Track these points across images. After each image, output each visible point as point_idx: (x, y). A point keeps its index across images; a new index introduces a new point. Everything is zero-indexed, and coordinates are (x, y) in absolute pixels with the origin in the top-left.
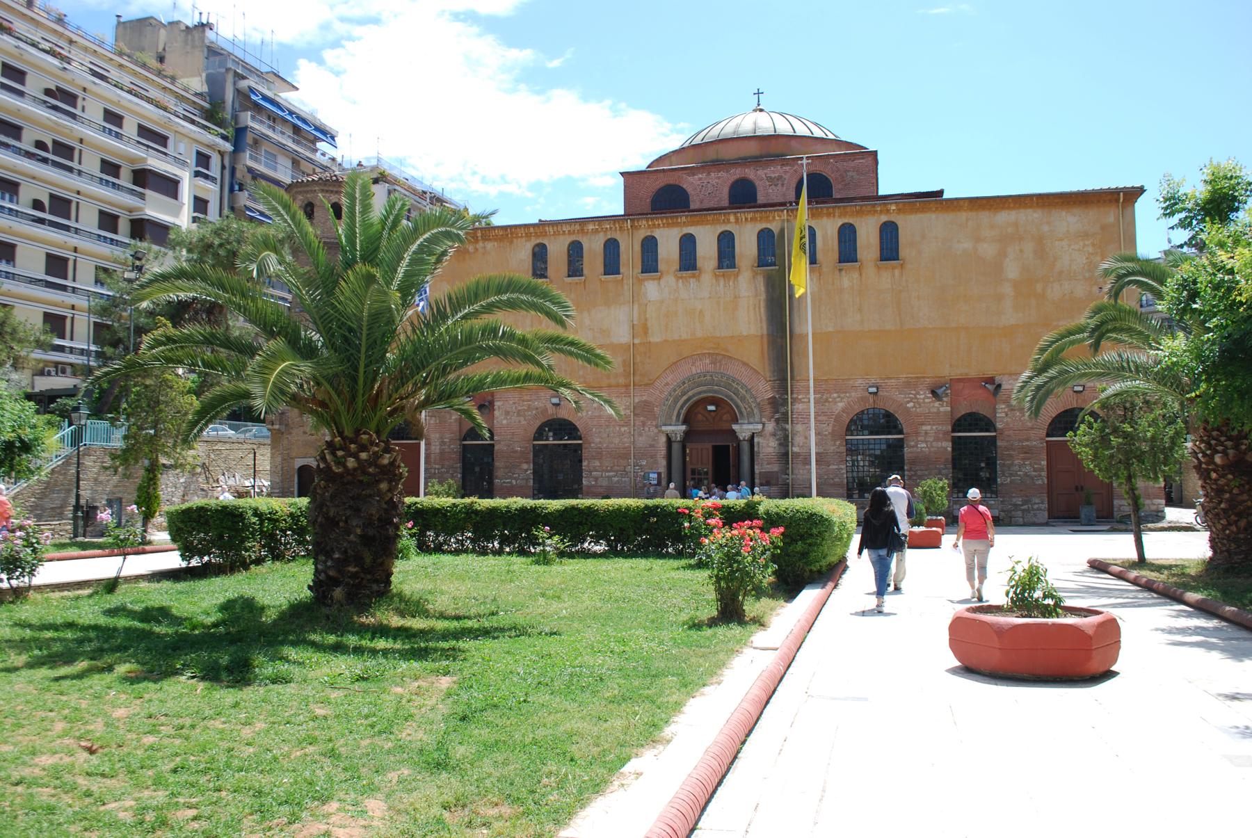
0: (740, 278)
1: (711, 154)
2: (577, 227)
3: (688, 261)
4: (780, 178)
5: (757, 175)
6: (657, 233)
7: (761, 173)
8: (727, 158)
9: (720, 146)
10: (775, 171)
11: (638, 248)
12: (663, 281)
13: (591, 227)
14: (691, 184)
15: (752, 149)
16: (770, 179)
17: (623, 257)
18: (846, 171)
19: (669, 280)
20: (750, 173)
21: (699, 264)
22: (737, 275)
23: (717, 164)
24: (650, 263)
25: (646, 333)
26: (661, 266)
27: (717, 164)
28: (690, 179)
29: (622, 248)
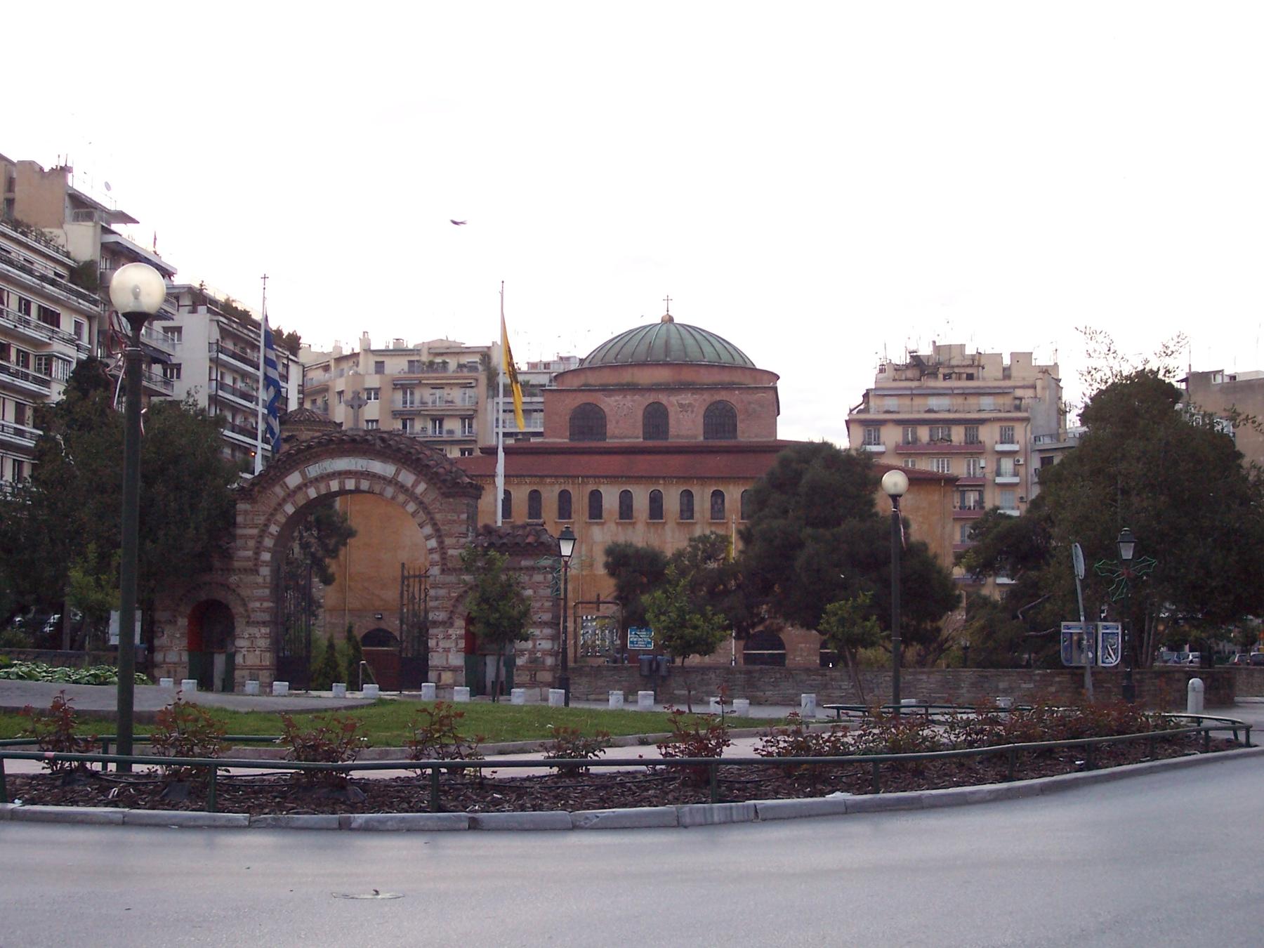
0: (667, 527)
1: (627, 376)
2: (538, 480)
3: (626, 510)
4: (690, 405)
5: (671, 402)
6: (602, 489)
7: (674, 399)
8: (641, 382)
9: (636, 370)
10: (686, 398)
11: (586, 500)
12: (606, 527)
13: (548, 480)
14: (610, 404)
15: (663, 375)
16: (681, 406)
17: (574, 506)
18: (749, 403)
19: (613, 526)
20: (663, 398)
21: (635, 514)
22: (665, 523)
23: (632, 388)
24: (596, 510)
25: (591, 565)
26: (604, 514)
27: (632, 388)
28: (607, 399)
29: (574, 499)
